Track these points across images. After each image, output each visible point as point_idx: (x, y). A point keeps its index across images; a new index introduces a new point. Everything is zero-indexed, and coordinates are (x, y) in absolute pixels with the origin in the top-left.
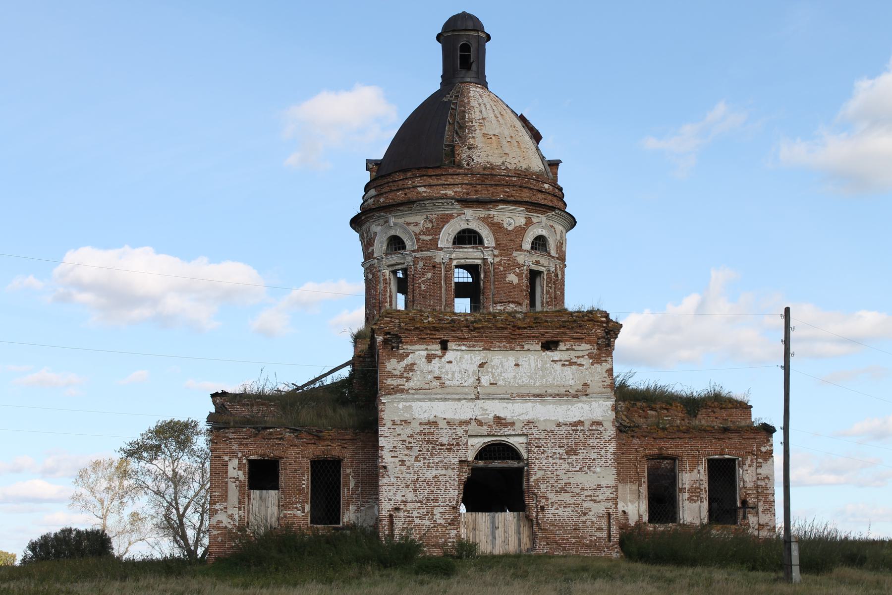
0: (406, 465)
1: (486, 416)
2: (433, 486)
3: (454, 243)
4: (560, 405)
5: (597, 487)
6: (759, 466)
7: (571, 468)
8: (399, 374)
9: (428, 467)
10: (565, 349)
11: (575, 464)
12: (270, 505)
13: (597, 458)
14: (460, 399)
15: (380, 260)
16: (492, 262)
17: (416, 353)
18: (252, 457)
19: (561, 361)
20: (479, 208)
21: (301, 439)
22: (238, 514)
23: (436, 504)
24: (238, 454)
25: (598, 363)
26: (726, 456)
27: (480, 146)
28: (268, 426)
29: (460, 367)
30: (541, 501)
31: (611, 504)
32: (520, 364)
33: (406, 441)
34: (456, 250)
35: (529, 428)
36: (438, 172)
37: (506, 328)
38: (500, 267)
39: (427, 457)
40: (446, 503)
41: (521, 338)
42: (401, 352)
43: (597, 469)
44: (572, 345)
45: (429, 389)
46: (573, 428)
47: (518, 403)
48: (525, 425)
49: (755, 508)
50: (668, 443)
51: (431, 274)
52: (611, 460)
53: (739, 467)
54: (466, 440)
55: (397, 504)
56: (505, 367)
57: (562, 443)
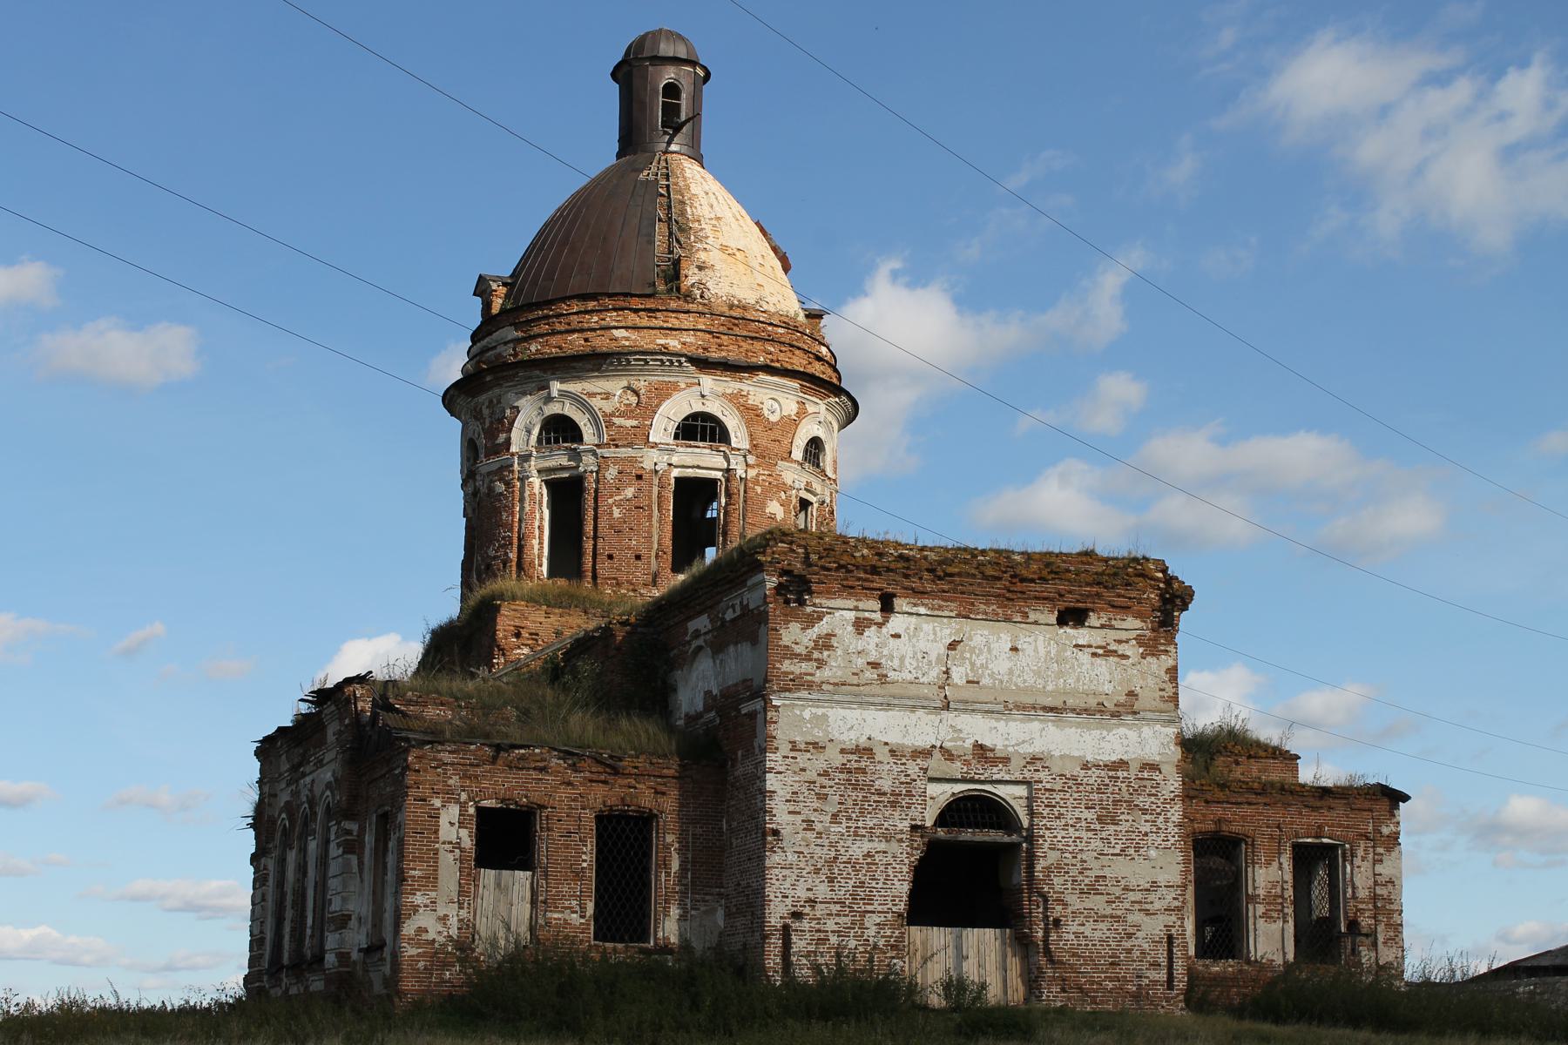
0: (814, 830)
1: (958, 743)
2: (864, 872)
3: (676, 437)
4: (1089, 729)
5: (1151, 886)
6: (1379, 861)
7: (1106, 849)
8: (804, 653)
9: (856, 834)
10: (1099, 625)
11: (1113, 842)
12: (515, 901)
13: (1151, 832)
14: (914, 707)
15: (525, 458)
16: (744, 476)
17: (837, 614)
18: (486, 803)
19: (1090, 646)
20: (726, 376)
21: (581, 772)
22: (457, 915)
23: (869, 908)
24: (459, 795)
25: (1153, 655)
26: (1325, 840)
27: (717, 267)
28: (518, 742)
29: (914, 646)
30: (1054, 908)
31: (1174, 918)
32: (1019, 647)
33: (815, 782)
34: (680, 449)
35: (1035, 770)
36: (650, 304)
37: (999, 579)
39: (854, 815)
40: (888, 906)
41: (1024, 598)
42: (809, 609)
43: (1152, 852)
44: (1110, 619)
45: (858, 685)
46: (1111, 773)
47: (1015, 720)
48: (1028, 763)
49: (1371, 935)
50: (1230, 812)
51: (633, 489)
52: (1174, 837)
53: (1344, 860)
54: (923, 786)
55: (798, 904)
56: (994, 653)
57: (1091, 800)
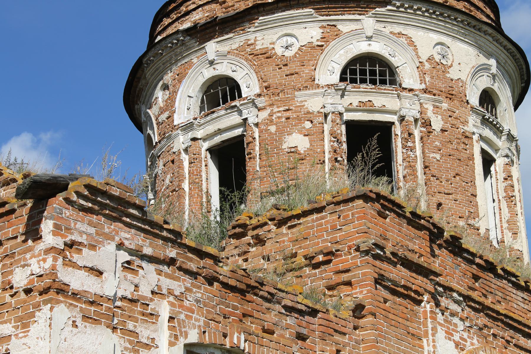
38: (269, 128)
